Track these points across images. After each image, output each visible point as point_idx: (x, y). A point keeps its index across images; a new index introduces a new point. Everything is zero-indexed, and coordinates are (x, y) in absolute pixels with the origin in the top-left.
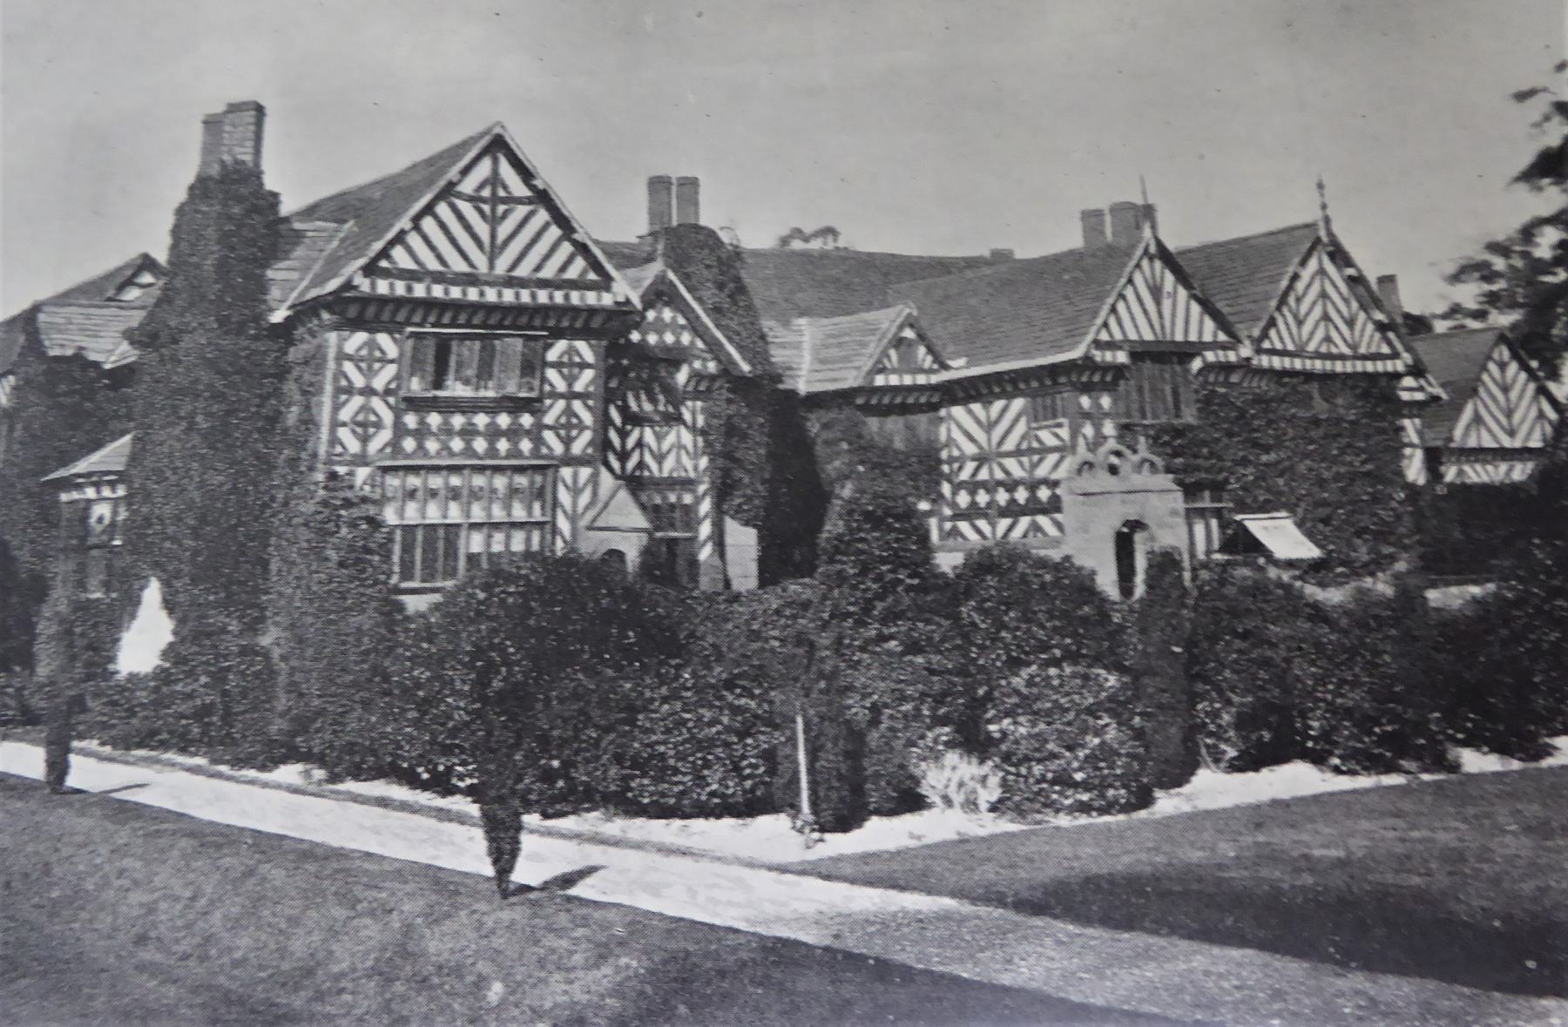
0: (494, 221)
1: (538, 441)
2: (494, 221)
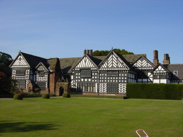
0: (20, 61)
1: (25, 78)
2: (20, 61)
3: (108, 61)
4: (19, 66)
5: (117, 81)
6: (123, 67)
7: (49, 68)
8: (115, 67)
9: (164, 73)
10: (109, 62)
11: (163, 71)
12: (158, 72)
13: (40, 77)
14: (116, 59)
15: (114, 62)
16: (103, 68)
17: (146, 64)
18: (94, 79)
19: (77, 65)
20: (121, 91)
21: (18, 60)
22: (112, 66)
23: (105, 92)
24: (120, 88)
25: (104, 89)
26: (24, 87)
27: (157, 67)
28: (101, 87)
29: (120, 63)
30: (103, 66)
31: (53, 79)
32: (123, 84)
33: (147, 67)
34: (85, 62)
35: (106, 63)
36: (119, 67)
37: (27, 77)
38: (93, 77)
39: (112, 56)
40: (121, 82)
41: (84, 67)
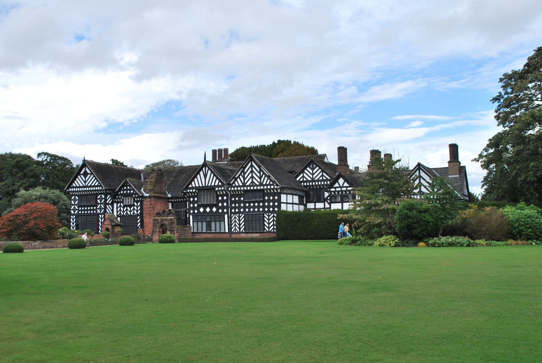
0: (85, 177)
1: (97, 211)
2: (85, 177)
3: (245, 174)
4: (83, 187)
5: (261, 209)
6: (271, 183)
7: (142, 189)
8: (258, 184)
9: (349, 191)
10: (246, 176)
11: (347, 187)
12: (337, 189)
13: (125, 208)
14: (258, 169)
15: (254, 175)
16: (236, 186)
17: (321, 174)
18: (223, 207)
19: (190, 183)
20: (269, 228)
21: (82, 176)
22: (252, 182)
23: (241, 230)
24: (267, 221)
25: (240, 225)
26: (96, 227)
27: (336, 180)
28: (235, 221)
29: (266, 175)
30: (236, 182)
31: (151, 211)
32: (272, 215)
33: (324, 181)
34: (205, 176)
35: (241, 177)
36: (264, 183)
37: (101, 209)
38: (220, 205)
39: (252, 163)
40: (269, 211)
41: (204, 185)
